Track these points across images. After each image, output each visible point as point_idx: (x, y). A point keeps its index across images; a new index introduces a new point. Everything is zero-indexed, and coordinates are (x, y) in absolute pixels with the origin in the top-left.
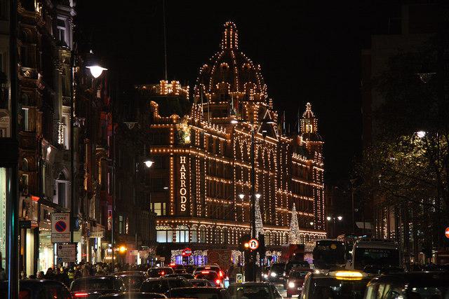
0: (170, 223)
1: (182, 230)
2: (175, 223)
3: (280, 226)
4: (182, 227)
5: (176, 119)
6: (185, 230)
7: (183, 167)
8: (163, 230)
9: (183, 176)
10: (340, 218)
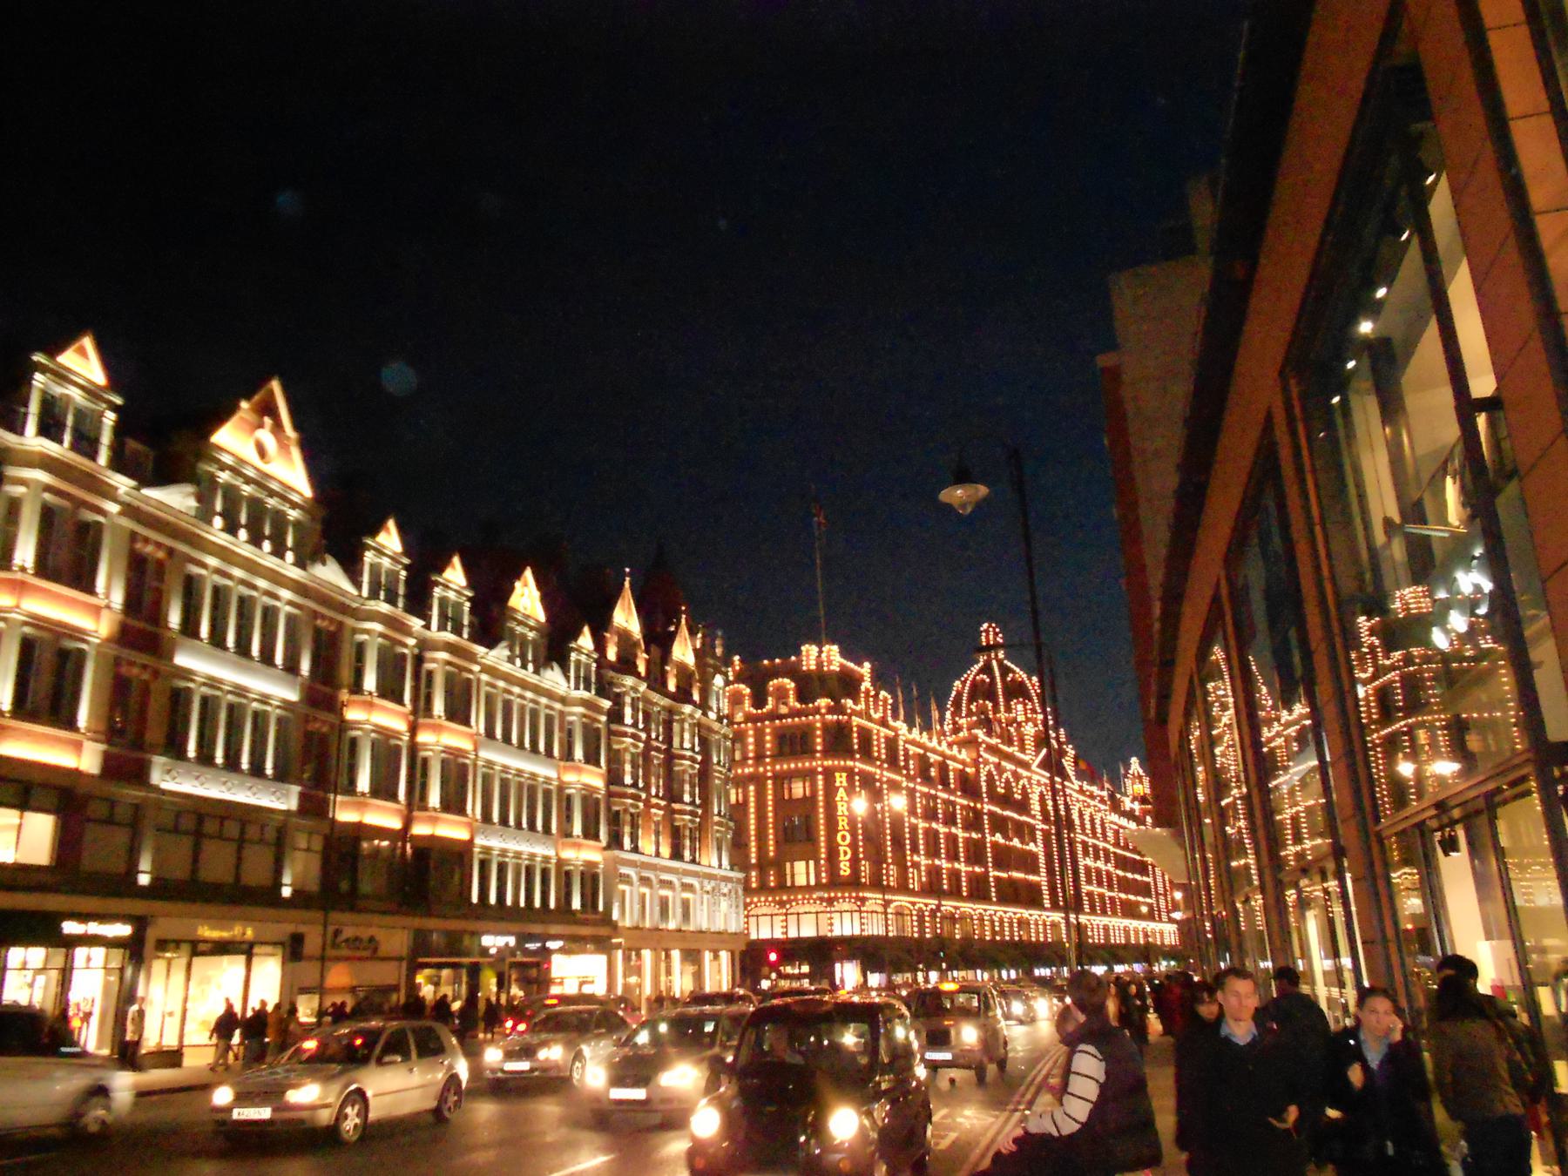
3: (1093, 911)
4: (846, 906)
5: (825, 707)
6: (852, 912)
8: (810, 913)
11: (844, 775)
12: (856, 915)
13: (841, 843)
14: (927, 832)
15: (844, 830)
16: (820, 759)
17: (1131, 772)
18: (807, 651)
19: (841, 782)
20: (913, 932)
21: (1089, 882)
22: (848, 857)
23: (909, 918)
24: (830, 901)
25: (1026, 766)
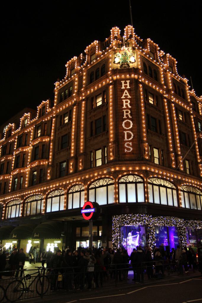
0: (109, 173)
1: (130, 183)
2: (116, 172)
4: (131, 178)
6: (136, 183)
7: (126, 93)
8: (103, 186)
9: (126, 104)
11: (128, 82)
12: (140, 186)
15: (128, 118)
16: (111, 76)
18: (113, 31)
19: (126, 86)
22: (130, 139)
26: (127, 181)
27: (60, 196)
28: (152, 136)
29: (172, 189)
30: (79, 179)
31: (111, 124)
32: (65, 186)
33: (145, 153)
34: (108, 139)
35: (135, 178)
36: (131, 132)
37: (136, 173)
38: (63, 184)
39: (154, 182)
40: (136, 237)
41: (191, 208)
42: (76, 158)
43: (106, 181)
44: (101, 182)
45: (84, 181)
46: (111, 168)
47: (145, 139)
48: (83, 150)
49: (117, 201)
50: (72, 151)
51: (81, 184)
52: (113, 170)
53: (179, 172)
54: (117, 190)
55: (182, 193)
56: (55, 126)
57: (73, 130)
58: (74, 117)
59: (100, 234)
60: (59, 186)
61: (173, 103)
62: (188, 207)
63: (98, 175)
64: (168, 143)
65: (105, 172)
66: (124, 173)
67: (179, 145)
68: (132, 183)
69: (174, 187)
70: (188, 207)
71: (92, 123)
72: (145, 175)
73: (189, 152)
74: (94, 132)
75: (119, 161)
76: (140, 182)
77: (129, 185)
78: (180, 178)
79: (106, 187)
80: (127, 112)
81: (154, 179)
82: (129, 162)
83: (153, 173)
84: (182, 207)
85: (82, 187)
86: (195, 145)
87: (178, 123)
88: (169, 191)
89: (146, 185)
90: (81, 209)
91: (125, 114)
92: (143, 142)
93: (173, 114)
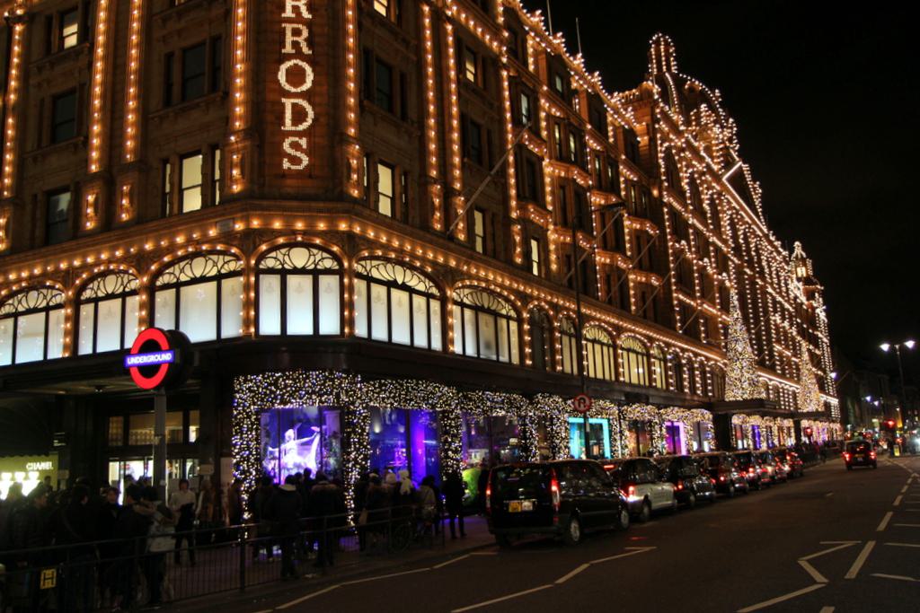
0: (228, 237)
1: (296, 271)
2: (249, 233)
4: (299, 258)
6: (316, 273)
10: (910, 344)
12: (329, 284)
13: (288, 87)
14: (563, 185)
15: (298, 54)
17: (794, 255)
20: (522, 356)
21: (778, 341)
22: (301, 127)
23: (514, 326)
24: (248, 242)
25: (717, 178)
26: (286, 266)
27: (47, 309)
28: (375, 125)
29: (428, 296)
30: (119, 253)
31: (239, 67)
32: (67, 278)
33: (349, 177)
34: (228, 120)
35: (312, 258)
36: (305, 104)
37: (318, 241)
38: (57, 270)
39: (375, 274)
40: (309, 443)
41: (481, 357)
42: (109, 181)
43: (215, 264)
44: (199, 268)
45: (138, 260)
46: (234, 221)
47: (352, 131)
48: (135, 151)
49: (252, 330)
50: (95, 155)
51: (126, 272)
52: (239, 226)
53: (452, 245)
54: (252, 295)
55: (456, 309)
56: (25, 56)
57: (98, 77)
58: (102, 27)
59: (193, 437)
60: (45, 275)
61: (451, 20)
62: (471, 351)
63: (189, 241)
64: (423, 152)
65: (212, 233)
66: (276, 237)
67: (457, 160)
68: (302, 271)
69: (434, 291)
70: (471, 351)
71: (169, 56)
72: (346, 248)
73: (487, 185)
74: (176, 89)
75: (263, 197)
76: (328, 272)
77: (292, 280)
78: (453, 263)
79: (214, 284)
80: (296, 32)
81: (375, 263)
82: (295, 204)
83: (373, 244)
84: (453, 353)
85: (129, 281)
86: (505, 165)
87: (462, 91)
88: (419, 301)
89: (346, 281)
90: (124, 353)
91: (289, 39)
92: (344, 140)
93: (447, 57)
